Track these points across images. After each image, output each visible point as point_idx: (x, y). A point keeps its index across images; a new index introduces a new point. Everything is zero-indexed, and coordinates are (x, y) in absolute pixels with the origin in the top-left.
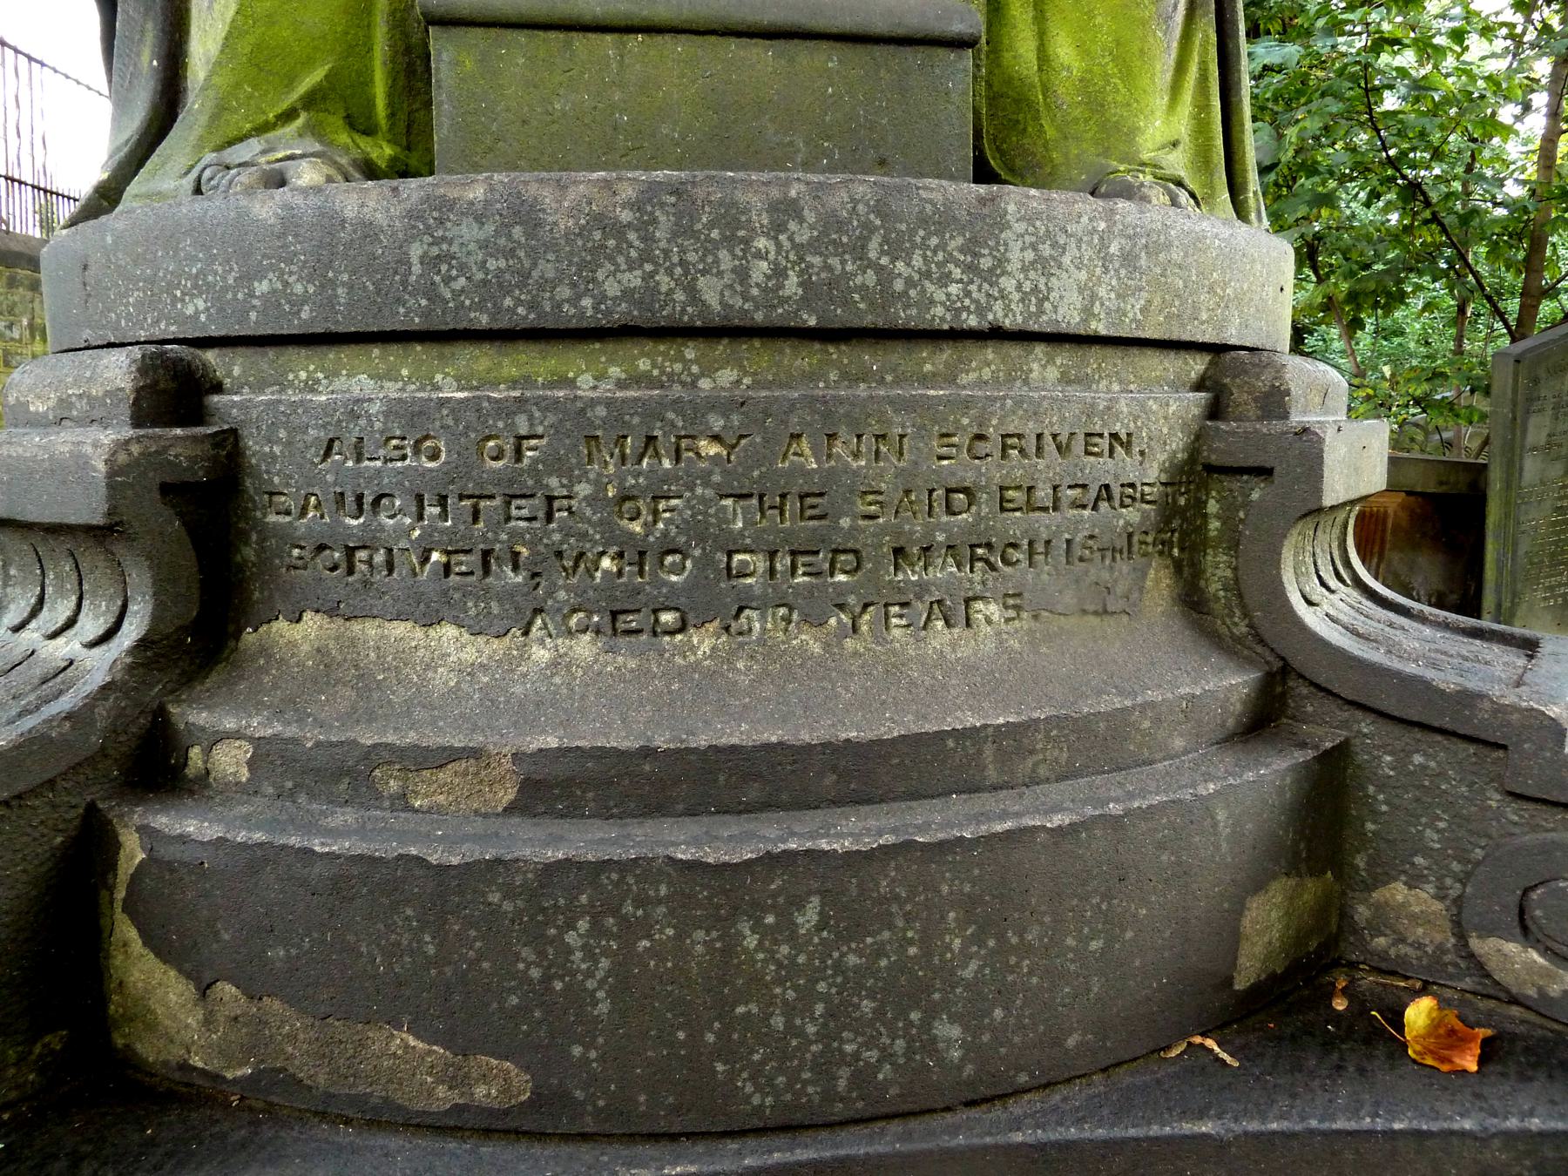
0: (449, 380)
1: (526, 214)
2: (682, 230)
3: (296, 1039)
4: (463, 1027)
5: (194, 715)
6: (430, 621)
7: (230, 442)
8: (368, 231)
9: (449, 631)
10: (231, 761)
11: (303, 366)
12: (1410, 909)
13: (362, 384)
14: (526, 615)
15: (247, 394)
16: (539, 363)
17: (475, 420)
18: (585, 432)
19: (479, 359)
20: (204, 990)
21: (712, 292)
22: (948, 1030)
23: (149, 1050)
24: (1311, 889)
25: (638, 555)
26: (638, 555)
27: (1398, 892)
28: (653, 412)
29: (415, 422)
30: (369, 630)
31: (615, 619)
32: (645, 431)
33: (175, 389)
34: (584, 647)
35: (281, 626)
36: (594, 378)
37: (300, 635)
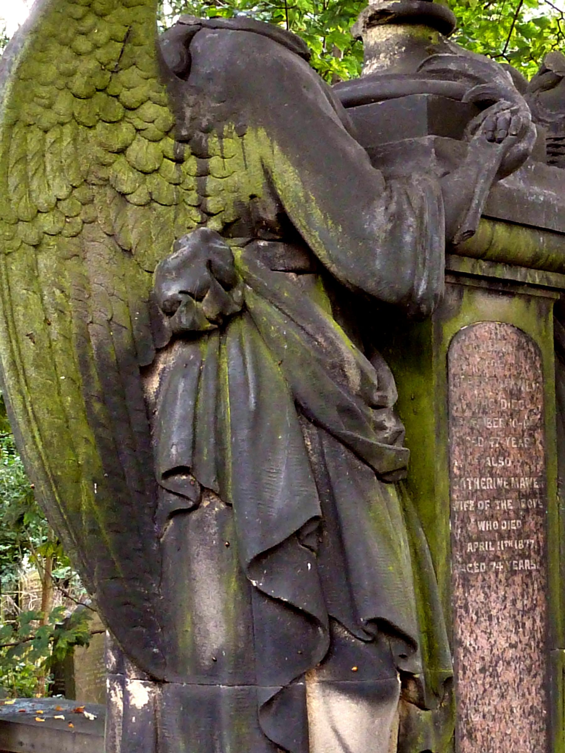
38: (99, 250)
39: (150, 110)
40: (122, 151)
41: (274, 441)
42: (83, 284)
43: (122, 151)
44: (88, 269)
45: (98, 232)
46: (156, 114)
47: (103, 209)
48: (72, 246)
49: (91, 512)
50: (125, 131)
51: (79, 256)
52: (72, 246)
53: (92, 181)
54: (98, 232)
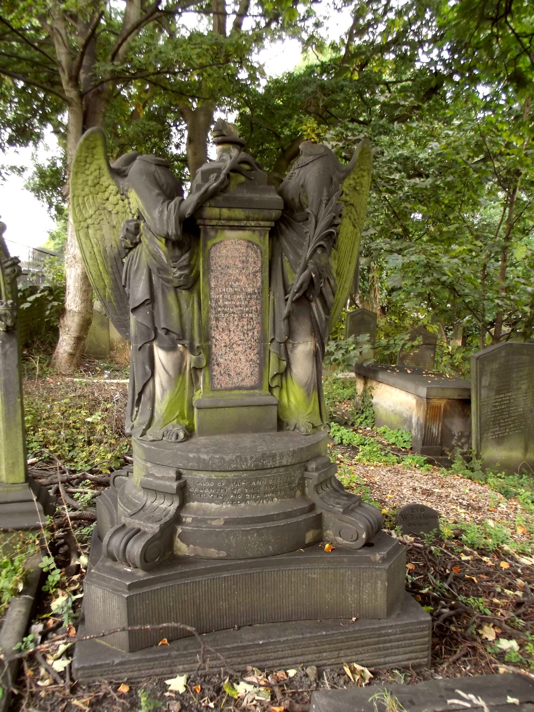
0: (213, 476)
1: (224, 459)
2: (241, 460)
3: (200, 551)
4: (219, 549)
5: (182, 514)
6: (211, 502)
7: (185, 482)
8: (204, 460)
9: (213, 504)
10: (189, 520)
11: (194, 473)
12: (329, 533)
13: (202, 475)
14: (222, 502)
15: (186, 475)
16: (224, 474)
17: (217, 481)
18: (229, 482)
19: (217, 474)
20: (188, 546)
21: (244, 467)
22: (270, 547)
23: (179, 553)
24: (317, 532)
25: (235, 495)
26: (235, 495)
27: (328, 532)
28: (237, 480)
29: (210, 480)
30: (203, 504)
31: (232, 502)
32: (236, 481)
33: (179, 476)
34: (229, 506)
35: (192, 503)
36: (230, 475)
37: (194, 504)
38: (106, 227)
39: (111, 187)
40: (107, 199)
41: (140, 278)
42: (103, 236)
43: (107, 199)
44: (104, 232)
45: (105, 223)
46: (113, 188)
47: (105, 216)
48: (97, 227)
49: (109, 297)
50: (107, 194)
51: (101, 229)
52: (97, 227)
53: (100, 208)
54: (105, 222)
